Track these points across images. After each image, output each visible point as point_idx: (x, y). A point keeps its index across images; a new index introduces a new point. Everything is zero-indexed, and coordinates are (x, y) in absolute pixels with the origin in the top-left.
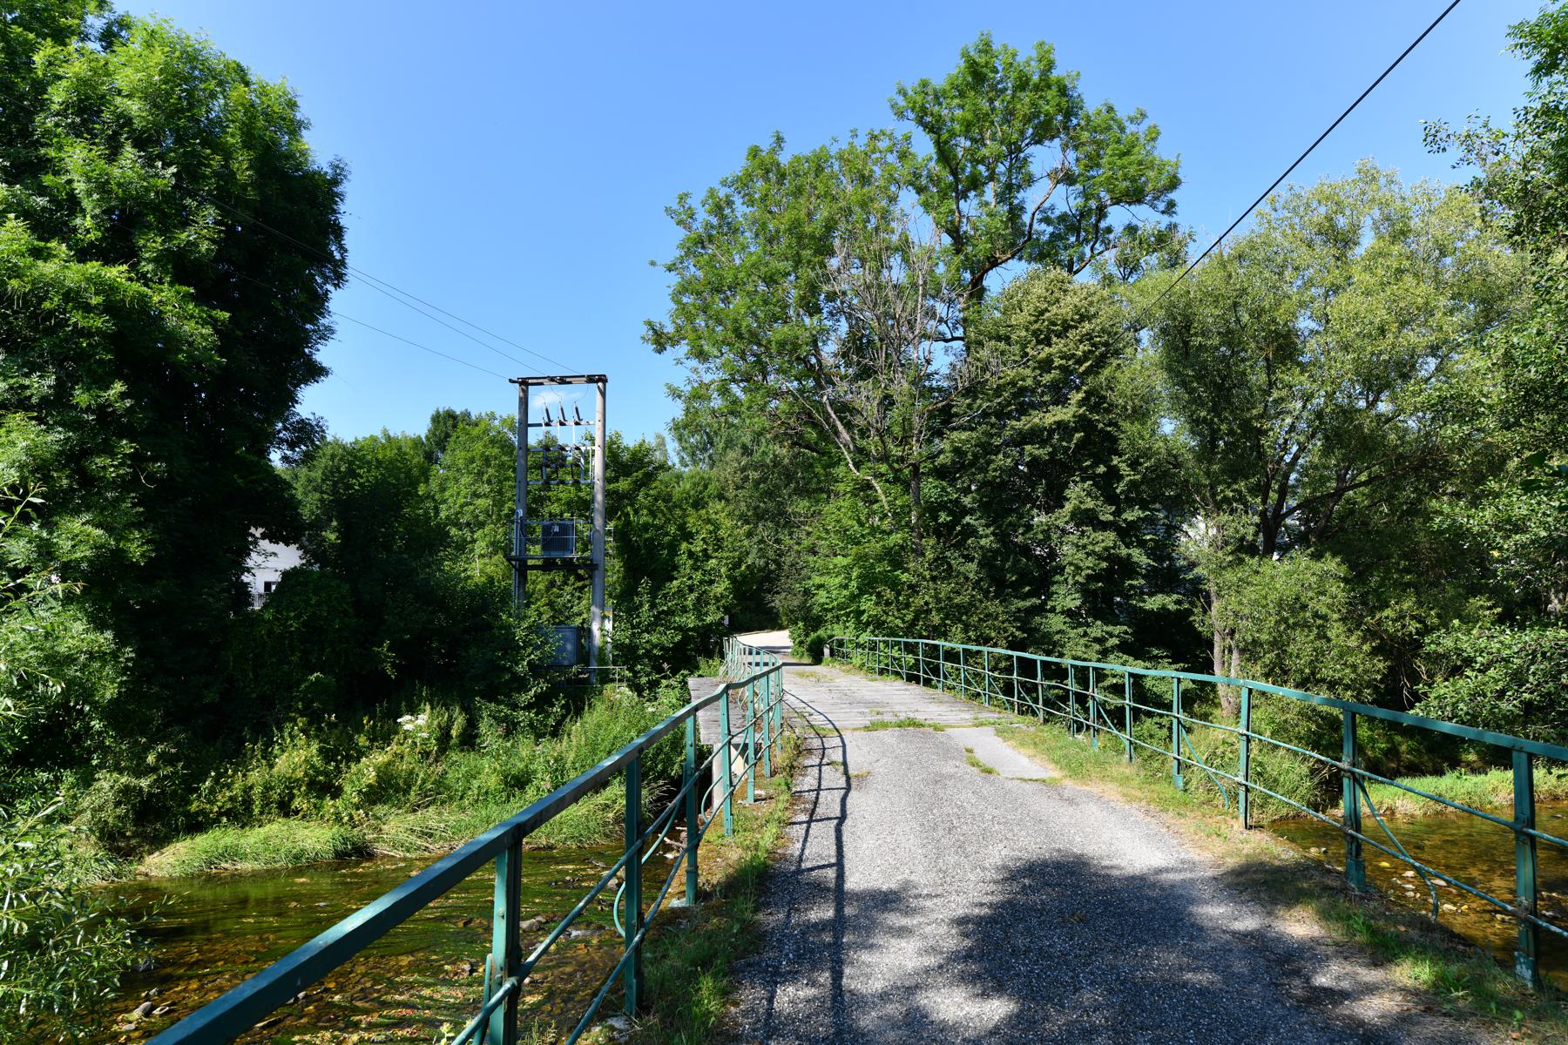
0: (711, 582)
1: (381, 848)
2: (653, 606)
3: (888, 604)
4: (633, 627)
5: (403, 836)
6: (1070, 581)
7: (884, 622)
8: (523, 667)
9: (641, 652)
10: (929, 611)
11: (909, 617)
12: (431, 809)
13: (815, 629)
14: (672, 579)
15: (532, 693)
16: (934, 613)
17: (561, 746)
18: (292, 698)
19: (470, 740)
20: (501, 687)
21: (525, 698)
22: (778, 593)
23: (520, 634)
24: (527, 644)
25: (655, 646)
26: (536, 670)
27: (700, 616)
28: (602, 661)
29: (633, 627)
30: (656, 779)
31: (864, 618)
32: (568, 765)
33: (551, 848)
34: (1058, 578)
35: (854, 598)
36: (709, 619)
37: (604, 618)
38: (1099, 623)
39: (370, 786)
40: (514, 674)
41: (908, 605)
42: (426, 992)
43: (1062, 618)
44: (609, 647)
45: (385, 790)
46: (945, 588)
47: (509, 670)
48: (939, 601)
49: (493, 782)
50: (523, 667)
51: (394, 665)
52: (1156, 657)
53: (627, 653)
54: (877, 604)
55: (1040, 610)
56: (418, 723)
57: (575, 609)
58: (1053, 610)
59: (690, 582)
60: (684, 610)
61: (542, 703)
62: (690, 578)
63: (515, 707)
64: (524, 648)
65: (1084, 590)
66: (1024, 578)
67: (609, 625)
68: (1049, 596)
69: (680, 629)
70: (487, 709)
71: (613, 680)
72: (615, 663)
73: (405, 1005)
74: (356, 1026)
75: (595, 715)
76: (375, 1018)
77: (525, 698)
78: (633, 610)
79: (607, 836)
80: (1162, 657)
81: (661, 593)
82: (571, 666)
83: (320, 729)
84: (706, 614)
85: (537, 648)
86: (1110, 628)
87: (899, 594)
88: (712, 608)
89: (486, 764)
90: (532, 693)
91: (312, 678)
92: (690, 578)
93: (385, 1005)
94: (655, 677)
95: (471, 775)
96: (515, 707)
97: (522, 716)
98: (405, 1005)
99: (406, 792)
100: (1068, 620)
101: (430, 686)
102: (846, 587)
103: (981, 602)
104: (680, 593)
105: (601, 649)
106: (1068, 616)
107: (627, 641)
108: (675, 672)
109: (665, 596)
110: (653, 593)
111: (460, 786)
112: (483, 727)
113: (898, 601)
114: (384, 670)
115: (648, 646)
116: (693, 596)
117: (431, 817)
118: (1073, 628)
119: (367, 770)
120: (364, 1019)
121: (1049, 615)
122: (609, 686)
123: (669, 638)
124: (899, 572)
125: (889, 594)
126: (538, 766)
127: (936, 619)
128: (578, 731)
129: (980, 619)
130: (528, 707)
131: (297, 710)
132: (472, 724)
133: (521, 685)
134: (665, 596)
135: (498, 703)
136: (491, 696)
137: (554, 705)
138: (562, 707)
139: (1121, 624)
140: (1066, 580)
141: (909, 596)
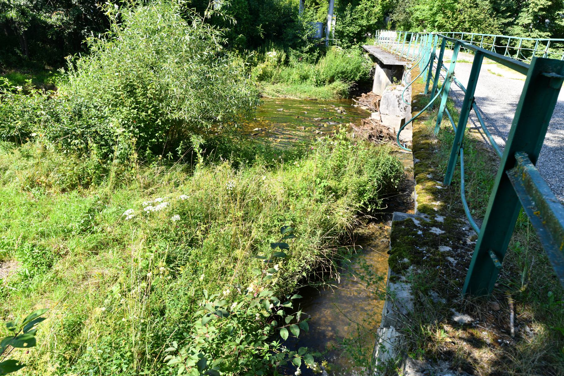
0: (374, 7)
1: (264, 95)
2: (351, 16)
3: (449, 18)
4: (343, 24)
5: (270, 92)
6: (530, 11)
7: (445, 26)
8: (305, 38)
9: (345, 34)
10: (464, 22)
11: (456, 24)
12: (278, 84)
13: (408, 29)
14: (359, 4)
15: (308, 47)
16: (467, 23)
17: (317, 67)
18: (233, 43)
19: (287, 63)
20: (297, 44)
21: (306, 49)
22: (395, 13)
23: (304, 24)
24: (307, 28)
25: (350, 32)
26: (310, 39)
27: (368, 21)
28: (330, 37)
29: (343, 24)
30: (350, 81)
31: (436, 24)
32: (321, 74)
33: (316, 100)
34: (524, 9)
35: (435, 14)
36: (371, 22)
37: (333, 20)
38: (537, 31)
39: (260, 75)
40: (302, 40)
41: (456, 19)
42: (294, 132)
43: (521, 28)
44: (334, 31)
45: (262, 78)
46: (475, 11)
47: (300, 38)
48: (470, 17)
49: (297, 77)
50: (305, 38)
51: (263, 34)
52: (558, 47)
53: (340, 35)
54: (443, 18)
55: (511, 24)
56: (272, 55)
57: (314, 17)
58: (517, 24)
59: (365, 6)
60: (362, 18)
61: (311, 51)
62: (366, 4)
63: (302, 52)
64: (306, 30)
65: (535, 15)
66: (509, 9)
67: (334, 23)
68: (517, 18)
69: (360, 26)
70: (293, 52)
71: (334, 45)
72: (335, 38)
73: (289, 134)
74: (278, 138)
75: (330, 55)
76: (282, 136)
77: (306, 49)
78: (343, 17)
79: (334, 98)
80: (560, 48)
81: (354, 10)
82: (320, 38)
83: (242, 55)
84: (370, 20)
85: (310, 30)
86: (541, 33)
87: (453, 14)
88: (373, 18)
89: (294, 70)
90: (308, 47)
91: (240, 36)
92: (366, 4)
93: (283, 134)
94: (349, 44)
95: (289, 75)
96: (302, 52)
97: (305, 55)
98: (289, 134)
99: (271, 78)
100: (523, 29)
101: (274, 42)
102: (431, 10)
103: (488, 18)
104: (362, 11)
105: (331, 32)
106: (524, 27)
107: (341, 30)
108: (358, 42)
109: (356, 11)
110: (352, 10)
111: (286, 77)
112: (291, 58)
113: (453, 17)
114: (260, 35)
115: (348, 32)
116: (367, 12)
117: (278, 86)
118: (524, 33)
119: (259, 69)
120: (280, 137)
121: (515, 26)
122: (333, 47)
123: (354, 29)
124: (456, 4)
125: (449, 14)
126: (311, 72)
127: (467, 25)
128: (324, 62)
129: (486, 26)
130: (307, 52)
131: (235, 48)
132: (287, 57)
133: (304, 43)
134: (356, 11)
135: (297, 50)
136: (294, 48)
137: (315, 52)
138: (318, 53)
139: (546, 31)
140: (528, 10)
141: (458, 15)
